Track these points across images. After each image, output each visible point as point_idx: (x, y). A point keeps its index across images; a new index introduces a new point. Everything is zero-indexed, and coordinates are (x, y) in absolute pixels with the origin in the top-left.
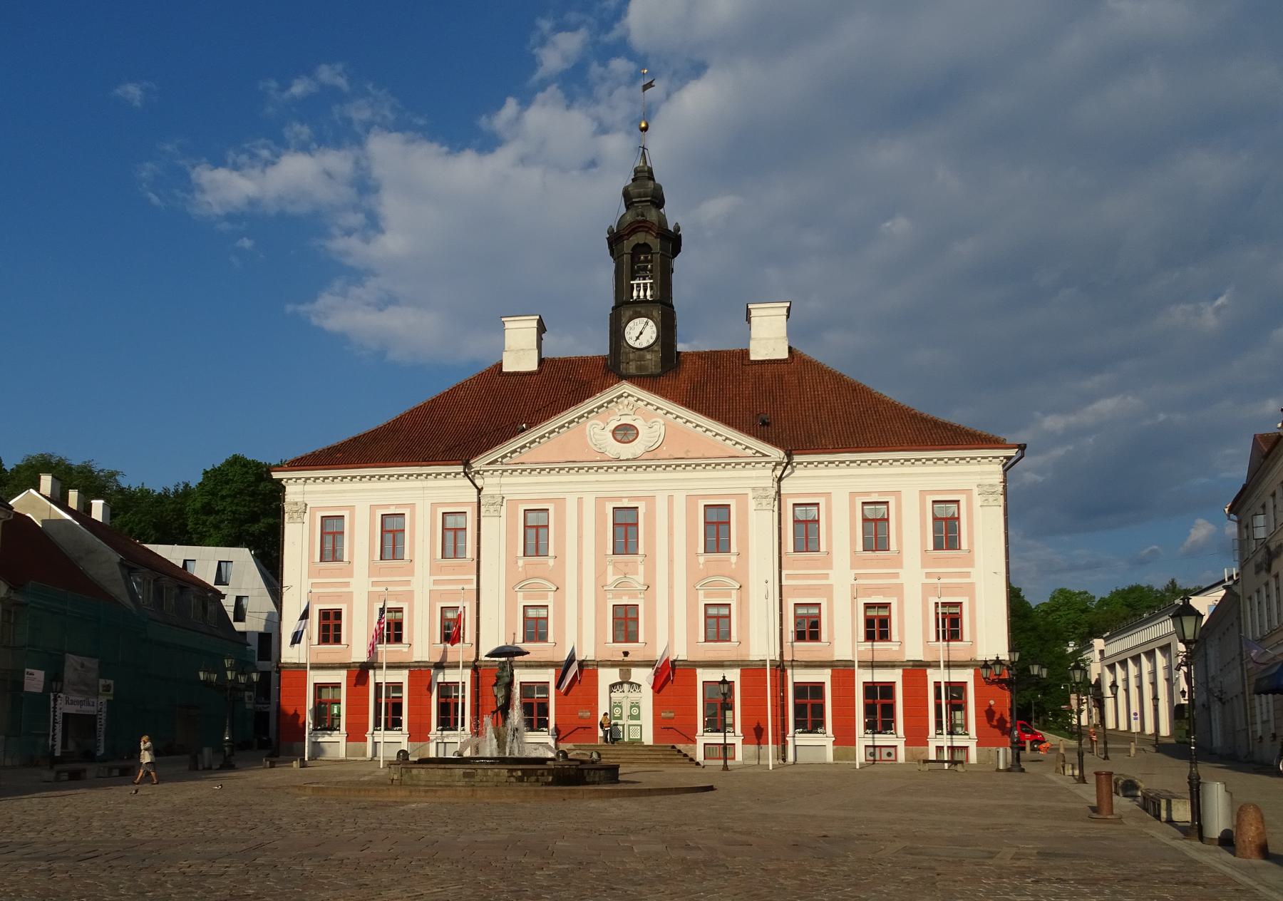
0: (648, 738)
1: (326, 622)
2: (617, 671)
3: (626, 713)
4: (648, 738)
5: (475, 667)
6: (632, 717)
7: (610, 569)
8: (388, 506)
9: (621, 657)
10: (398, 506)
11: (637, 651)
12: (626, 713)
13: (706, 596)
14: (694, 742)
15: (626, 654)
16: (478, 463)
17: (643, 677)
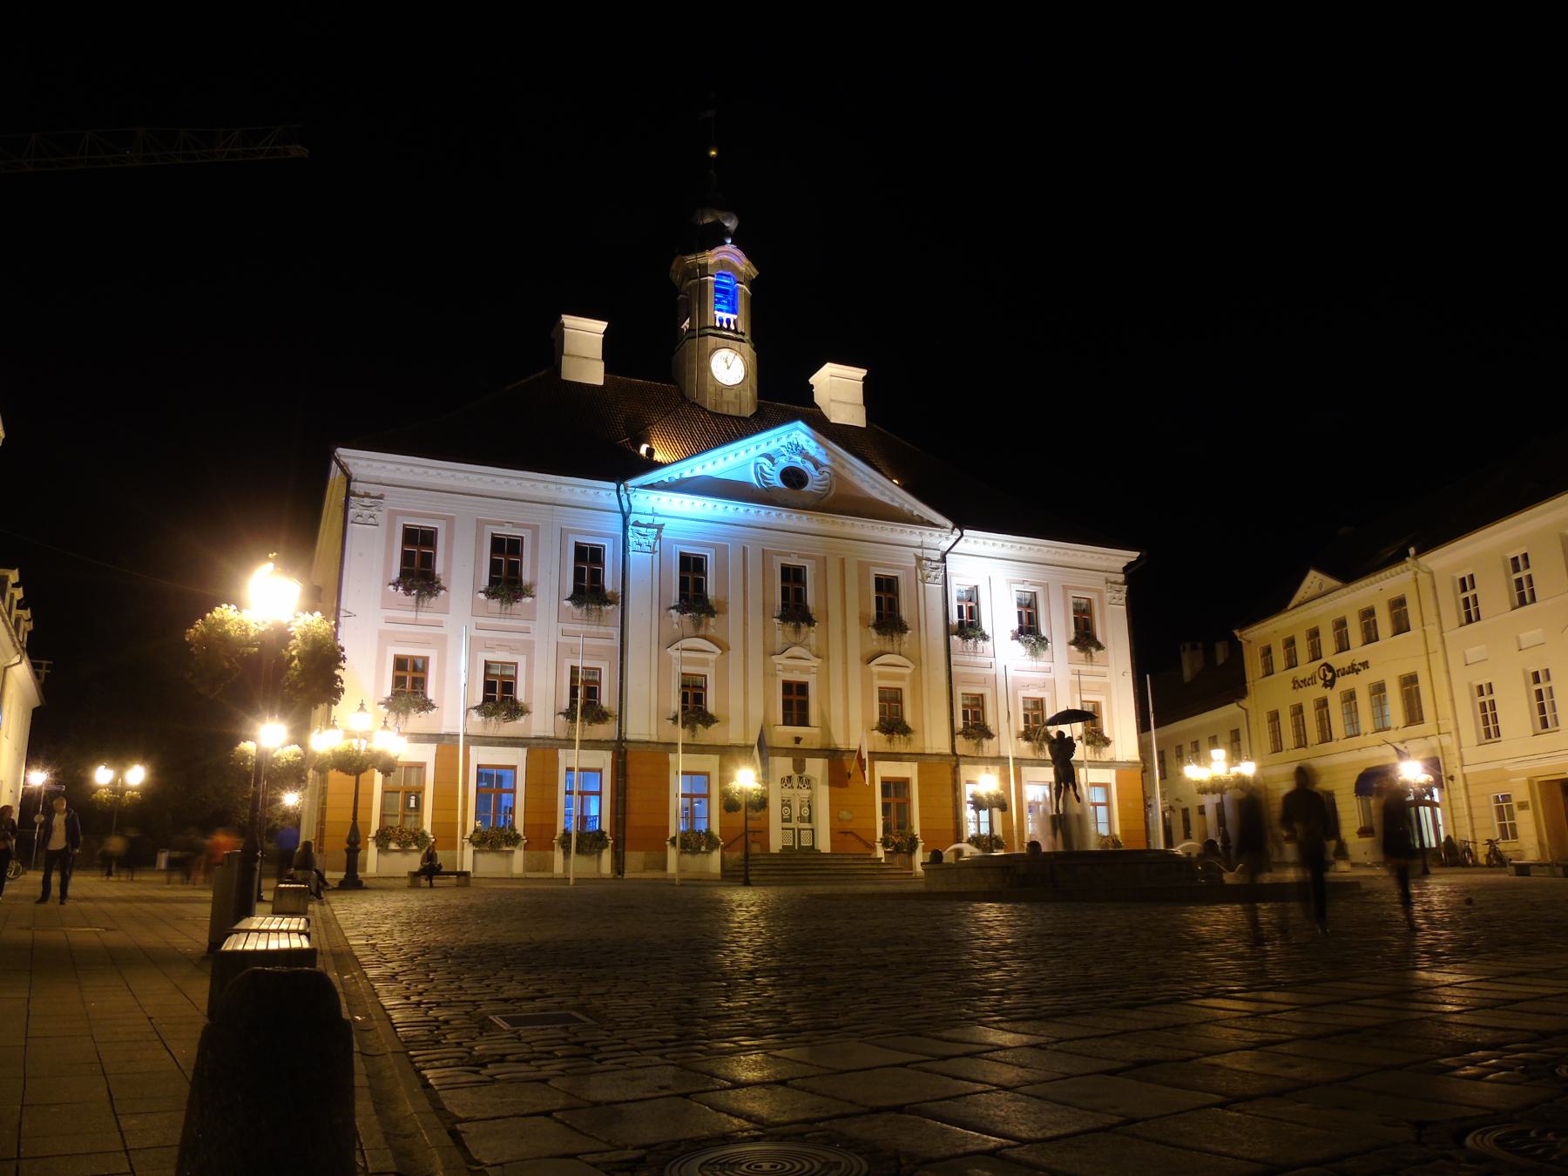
0: (824, 845)
1: (402, 674)
2: (788, 761)
3: (796, 814)
4: (824, 845)
5: (621, 750)
6: (801, 819)
7: (779, 634)
8: (501, 524)
9: (791, 744)
10: (515, 525)
11: (810, 735)
12: (796, 814)
13: (881, 676)
14: (874, 848)
15: (798, 740)
16: (631, 483)
17: (817, 768)
